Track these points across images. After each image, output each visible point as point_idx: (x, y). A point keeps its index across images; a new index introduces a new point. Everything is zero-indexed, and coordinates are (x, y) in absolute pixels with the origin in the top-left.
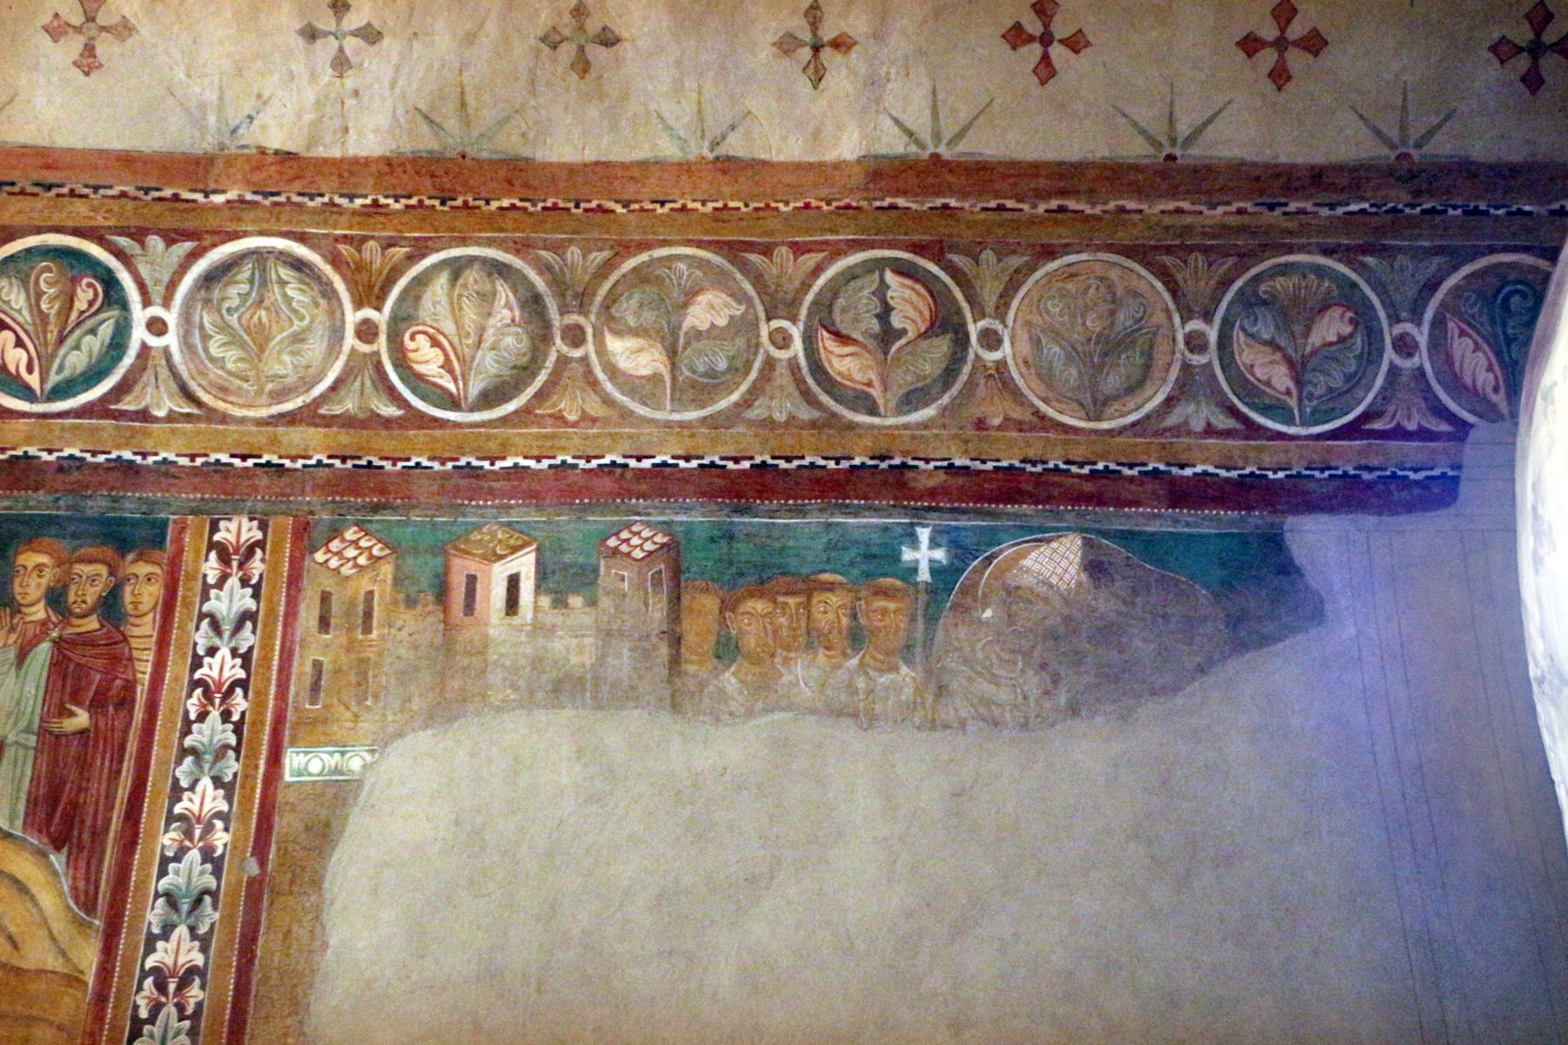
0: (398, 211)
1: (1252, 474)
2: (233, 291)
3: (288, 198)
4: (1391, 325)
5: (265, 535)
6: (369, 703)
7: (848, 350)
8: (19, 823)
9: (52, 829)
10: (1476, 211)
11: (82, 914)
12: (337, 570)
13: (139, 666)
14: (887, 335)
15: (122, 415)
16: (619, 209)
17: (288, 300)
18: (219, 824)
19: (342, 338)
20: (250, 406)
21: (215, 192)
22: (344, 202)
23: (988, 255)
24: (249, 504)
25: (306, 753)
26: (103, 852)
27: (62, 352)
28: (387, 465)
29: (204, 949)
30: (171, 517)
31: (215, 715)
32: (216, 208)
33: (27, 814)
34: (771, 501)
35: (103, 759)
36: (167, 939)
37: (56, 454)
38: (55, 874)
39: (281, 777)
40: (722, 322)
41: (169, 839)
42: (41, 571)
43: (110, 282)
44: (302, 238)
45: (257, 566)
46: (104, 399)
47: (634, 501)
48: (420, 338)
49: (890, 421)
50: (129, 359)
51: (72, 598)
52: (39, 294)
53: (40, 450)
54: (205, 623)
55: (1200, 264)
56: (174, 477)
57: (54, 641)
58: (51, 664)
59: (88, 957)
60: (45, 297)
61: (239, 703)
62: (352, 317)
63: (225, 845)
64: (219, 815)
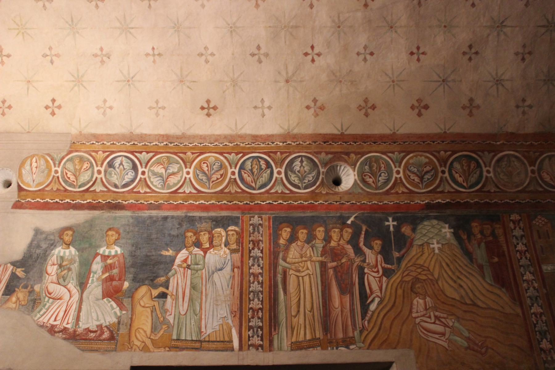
8: (493, 282)
12: (538, 225)
15: (484, 192)
18: (534, 282)
20: (511, 189)
22: (524, 143)
27: (470, 178)
29: (542, 308)
31: (524, 258)
36: (533, 306)
41: (525, 285)
44: (517, 151)
45: (522, 225)
46: (481, 188)
50: (484, 179)
52: (463, 165)
54: (514, 238)
59: (519, 310)
61: (528, 255)
62: (530, 169)
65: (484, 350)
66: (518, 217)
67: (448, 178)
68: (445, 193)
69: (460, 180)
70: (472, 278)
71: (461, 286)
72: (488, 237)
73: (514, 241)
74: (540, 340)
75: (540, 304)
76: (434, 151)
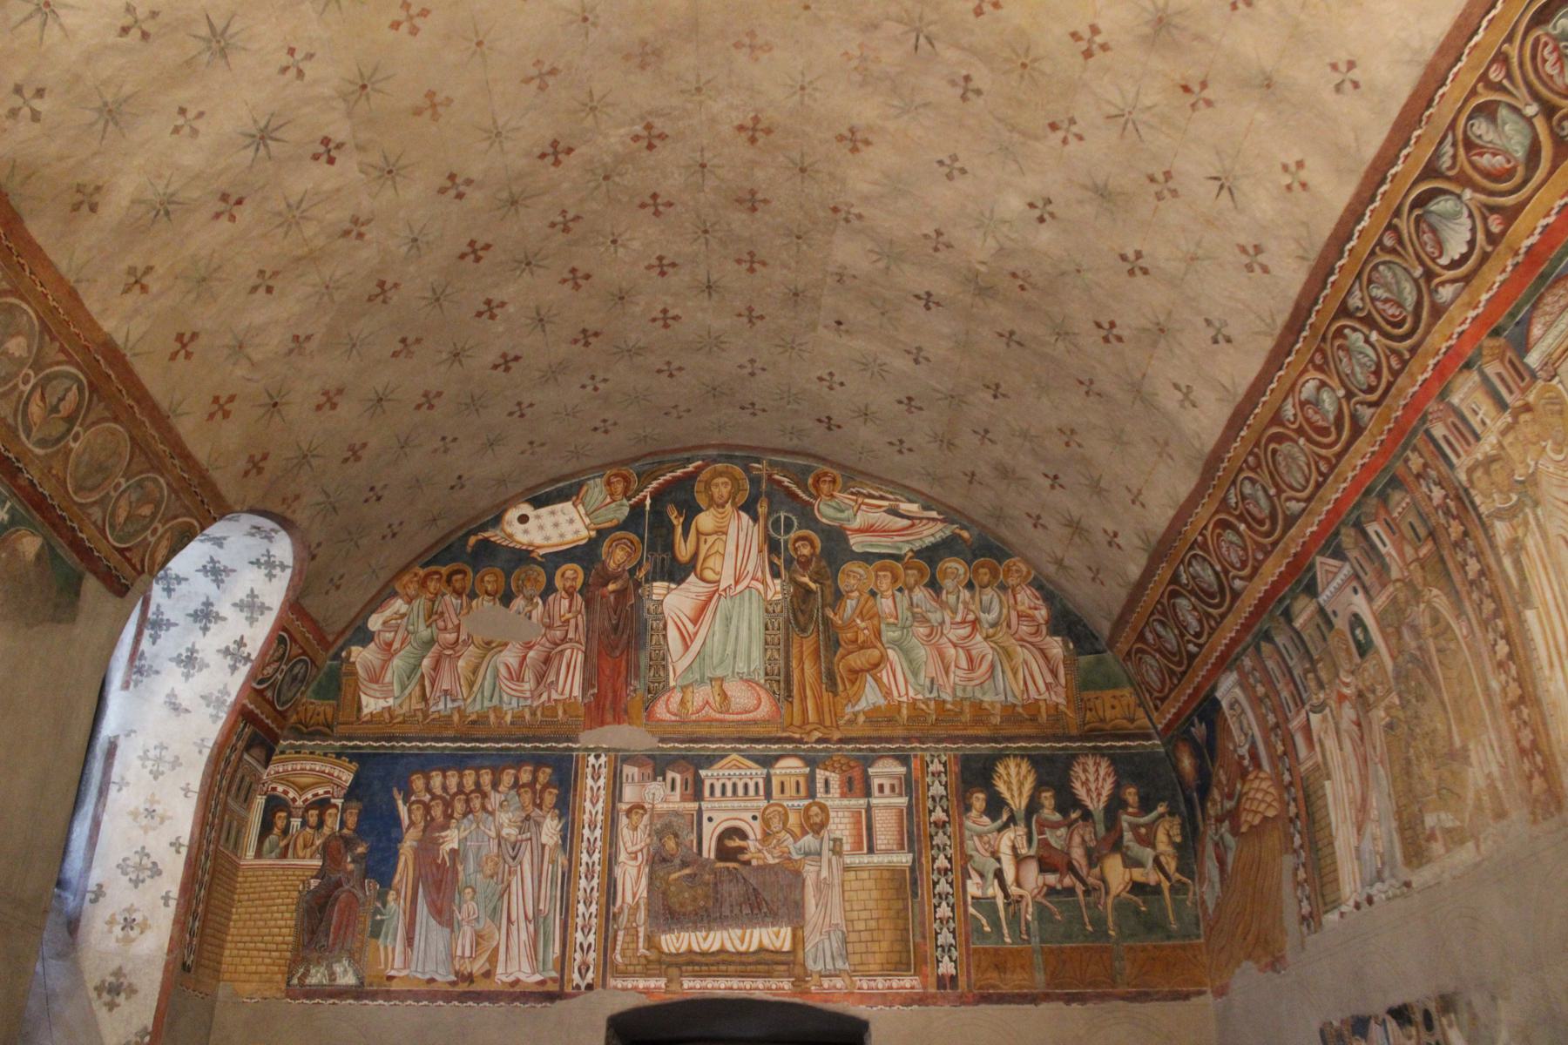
7: (41, 404)
14: (55, 409)
16: (27, 273)
40: (17, 354)
49: (30, 446)
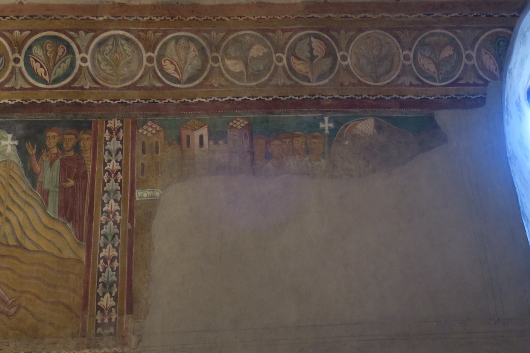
0: (158, 22)
1: (424, 98)
2: (107, 48)
3: (123, 18)
4: (465, 51)
5: (123, 125)
6: (160, 175)
7: (301, 62)
8: (57, 214)
9: (67, 216)
10: (490, 16)
11: (79, 241)
12: (146, 135)
13: (87, 166)
14: (312, 57)
15: (75, 88)
16: (227, 19)
17: (125, 50)
18: (117, 213)
19: (142, 62)
20: (115, 84)
21: (100, 17)
22: (141, 19)
23: (343, 32)
24: (117, 115)
25: (142, 191)
26: (83, 222)
27: (55, 69)
28: (159, 102)
29: (117, 251)
30: (93, 120)
31: (112, 180)
32: (101, 22)
33: (58, 212)
34: (279, 110)
35: (80, 194)
37: (56, 101)
38: (70, 229)
39: (135, 198)
40: (261, 54)
41: (103, 218)
42: (54, 138)
43: (69, 47)
44: (128, 31)
45: (121, 134)
46: (69, 83)
47: (237, 111)
48: (167, 61)
49: (314, 84)
50: (76, 71)
51: (65, 146)
52: (47, 51)
53: (51, 100)
54: (107, 152)
55: (407, 33)
56: (93, 107)
57: (60, 159)
58: (60, 166)
59: (83, 255)
60: (48, 52)
61: (120, 177)
62: (145, 55)
63: (120, 220)
64: (117, 211)
65: (12, 311)
66: (118, 124)
67: (24, 69)
68: (16, 90)
69: (41, 71)
70: (26, 208)
71: (8, 221)
72: (67, 151)
73: (106, 157)
74: (101, 295)
75: (116, 245)
76: (5, 30)
